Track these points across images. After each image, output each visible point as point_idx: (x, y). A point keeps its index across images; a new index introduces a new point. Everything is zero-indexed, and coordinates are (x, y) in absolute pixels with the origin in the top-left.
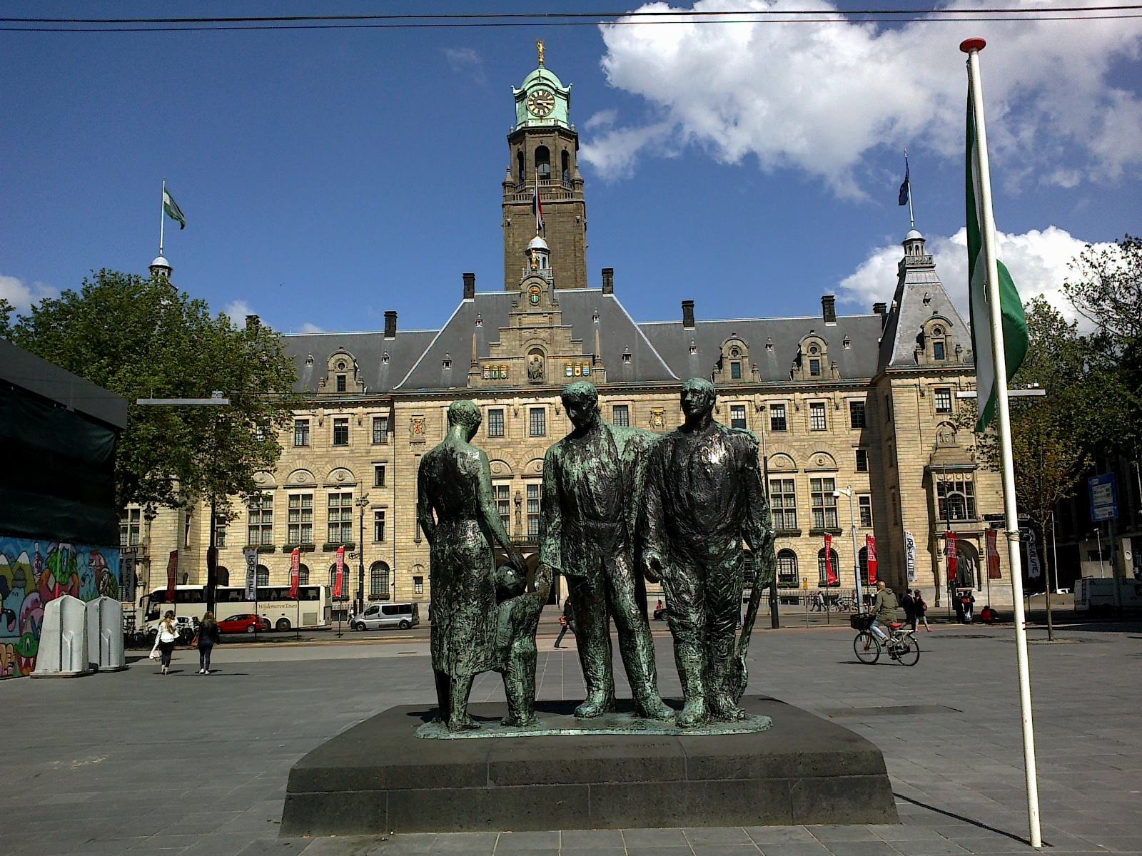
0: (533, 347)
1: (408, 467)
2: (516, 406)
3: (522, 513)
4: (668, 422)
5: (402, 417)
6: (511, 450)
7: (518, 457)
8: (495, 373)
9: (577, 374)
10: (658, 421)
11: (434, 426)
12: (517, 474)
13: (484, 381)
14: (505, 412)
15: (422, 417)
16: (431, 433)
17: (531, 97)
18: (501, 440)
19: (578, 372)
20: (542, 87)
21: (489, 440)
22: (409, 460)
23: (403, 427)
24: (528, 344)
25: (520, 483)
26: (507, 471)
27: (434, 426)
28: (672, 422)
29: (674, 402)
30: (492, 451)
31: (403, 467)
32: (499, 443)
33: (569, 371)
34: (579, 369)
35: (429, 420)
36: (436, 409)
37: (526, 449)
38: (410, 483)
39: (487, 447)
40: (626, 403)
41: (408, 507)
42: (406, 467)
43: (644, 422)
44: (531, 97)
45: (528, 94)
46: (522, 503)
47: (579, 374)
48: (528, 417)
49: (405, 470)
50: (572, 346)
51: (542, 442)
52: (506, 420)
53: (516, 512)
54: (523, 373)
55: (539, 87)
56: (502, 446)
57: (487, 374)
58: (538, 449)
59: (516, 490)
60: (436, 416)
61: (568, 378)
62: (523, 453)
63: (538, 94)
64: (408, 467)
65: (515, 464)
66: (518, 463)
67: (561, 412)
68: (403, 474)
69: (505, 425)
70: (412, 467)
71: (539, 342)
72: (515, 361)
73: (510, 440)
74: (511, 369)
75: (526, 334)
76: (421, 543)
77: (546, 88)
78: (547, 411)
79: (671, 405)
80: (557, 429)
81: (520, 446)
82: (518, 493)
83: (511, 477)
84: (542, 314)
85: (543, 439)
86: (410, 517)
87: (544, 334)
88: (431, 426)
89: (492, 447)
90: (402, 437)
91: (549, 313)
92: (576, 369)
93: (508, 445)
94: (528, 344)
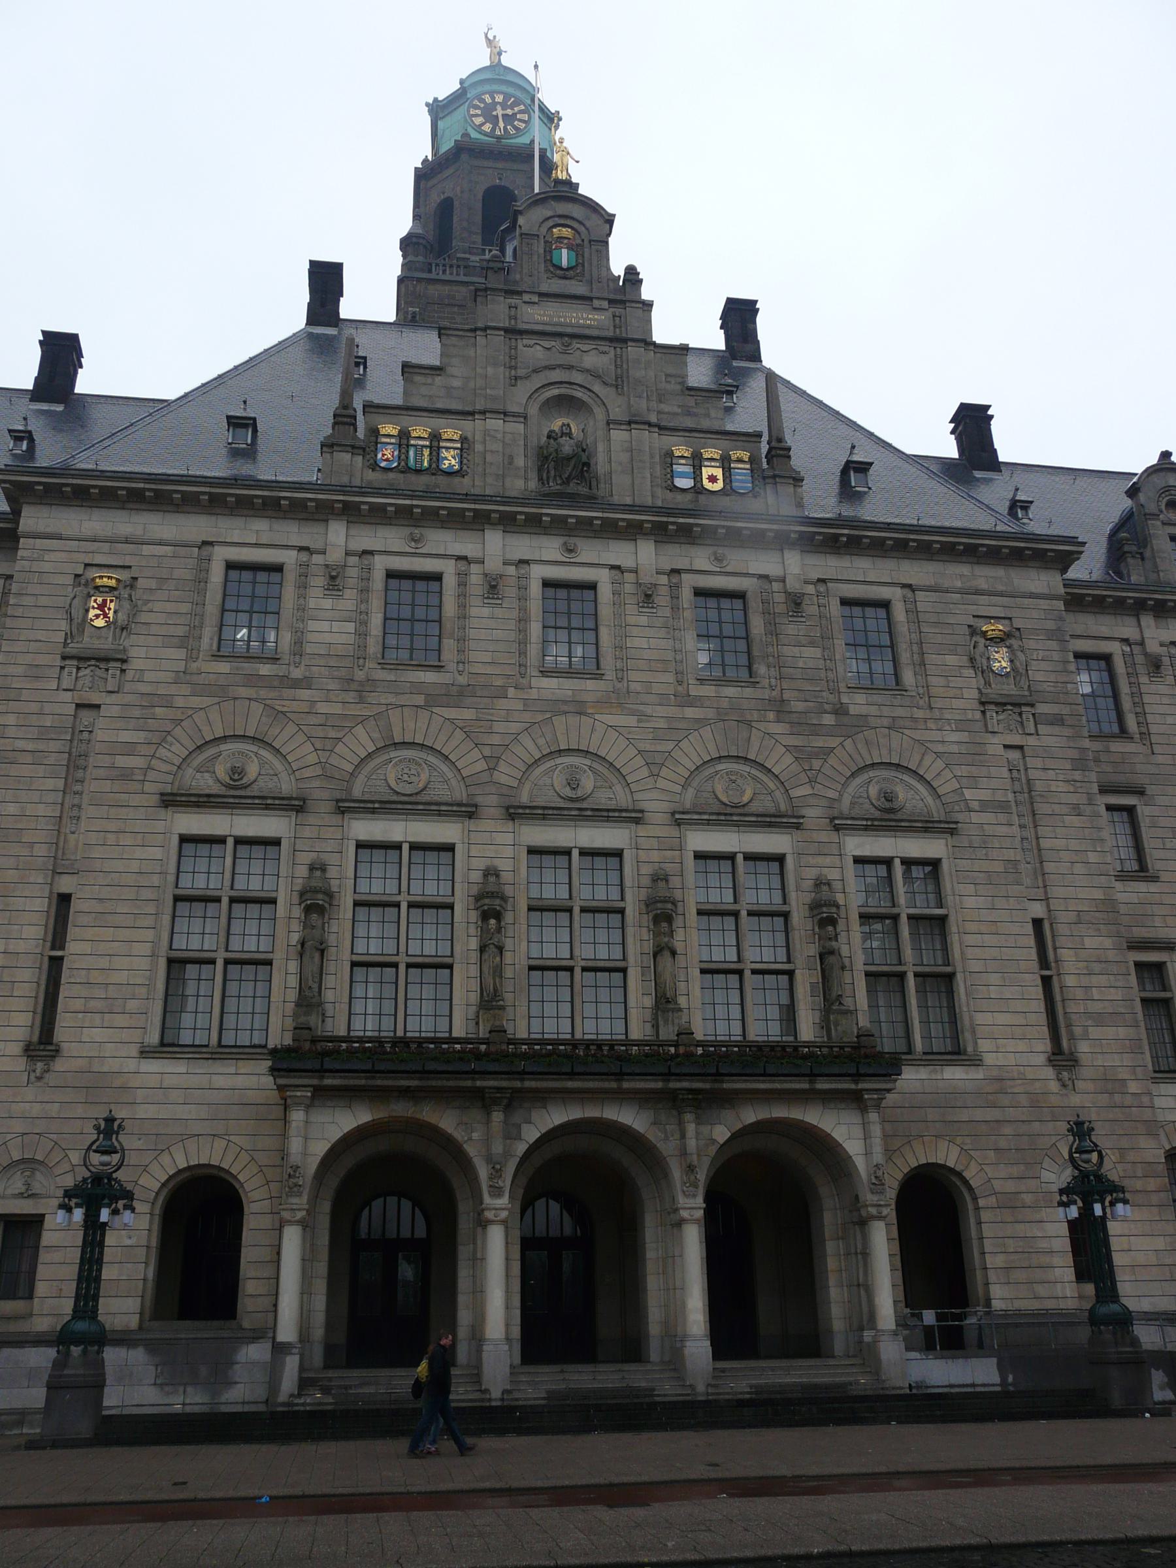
0: (555, 391)
1: (41, 746)
2: (493, 565)
3: (508, 957)
4: (1034, 665)
5: (46, 567)
6: (468, 714)
7: (496, 739)
8: (419, 450)
9: (707, 485)
10: (1001, 660)
11: (169, 607)
12: (489, 801)
13: (371, 475)
14: (450, 581)
15: (124, 575)
16: (154, 629)
17: (476, 102)
18: (430, 677)
19: (713, 479)
20: (504, 88)
21: (381, 675)
22: (48, 722)
23: (43, 601)
24: (538, 381)
25: (500, 838)
26: (450, 789)
27: (169, 607)
28: (1044, 665)
29: (1044, 604)
30: (394, 716)
31: (20, 744)
32: (417, 688)
33: (683, 475)
34: (718, 472)
35: (153, 584)
36: (182, 551)
37: (527, 717)
38: (41, 810)
39: (372, 698)
40: (884, 593)
41: (18, 903)
42: (30, 746)
43: (951, 660)
44: (476, 102)
45: (469, 96)
46: (508, 917)
47: (718, 486)
48: (535, 606)
49: (29, 758)
50: (691, 401)
51: (589, 698)
52: (450, 607)
53: (482, 949)
54: (520, 462)
55: (495, 87)
56: (434, 699)
57: (387, 454)
58: (573, 720)
59: (481, 864)
60: (177, 574)
61: (679, 497)
62: (514, 727)
63: (493, 98)
64: (41, 746)
65: (482, 765)
66: (493, 762)
67: (658, 600)
68: (14, 770)
69: (447, 625)
70: (53, 746)
71: (578, 378)
72: (494, 424)
73: (462, 680)
74: (479, 447)
75: (534, 352)
76: (59, 1065)
77: (511, 90)
78: (605, 591)
79: (1035, 614)
80: (646, 655)
81: (502, 704)
82: (491, 873)
83: (468, 811)
84: (591, 299)
85: (590, 684)
86: (21, 946)
87: (595, 359)
88: (157, 606)
89: (392, 699)
90: (32, 635)
91: (611, 301)
92: (706, 472)
93: (455, 696)
94: (538, 381)
